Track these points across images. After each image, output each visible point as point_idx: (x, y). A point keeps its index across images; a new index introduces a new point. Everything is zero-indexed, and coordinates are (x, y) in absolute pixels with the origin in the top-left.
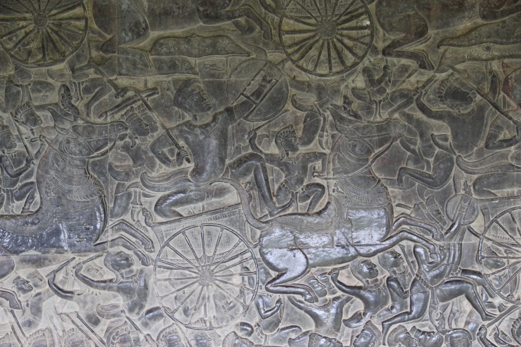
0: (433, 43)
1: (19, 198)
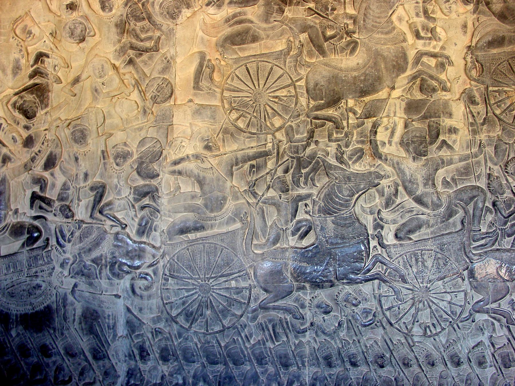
1: (509, 236)
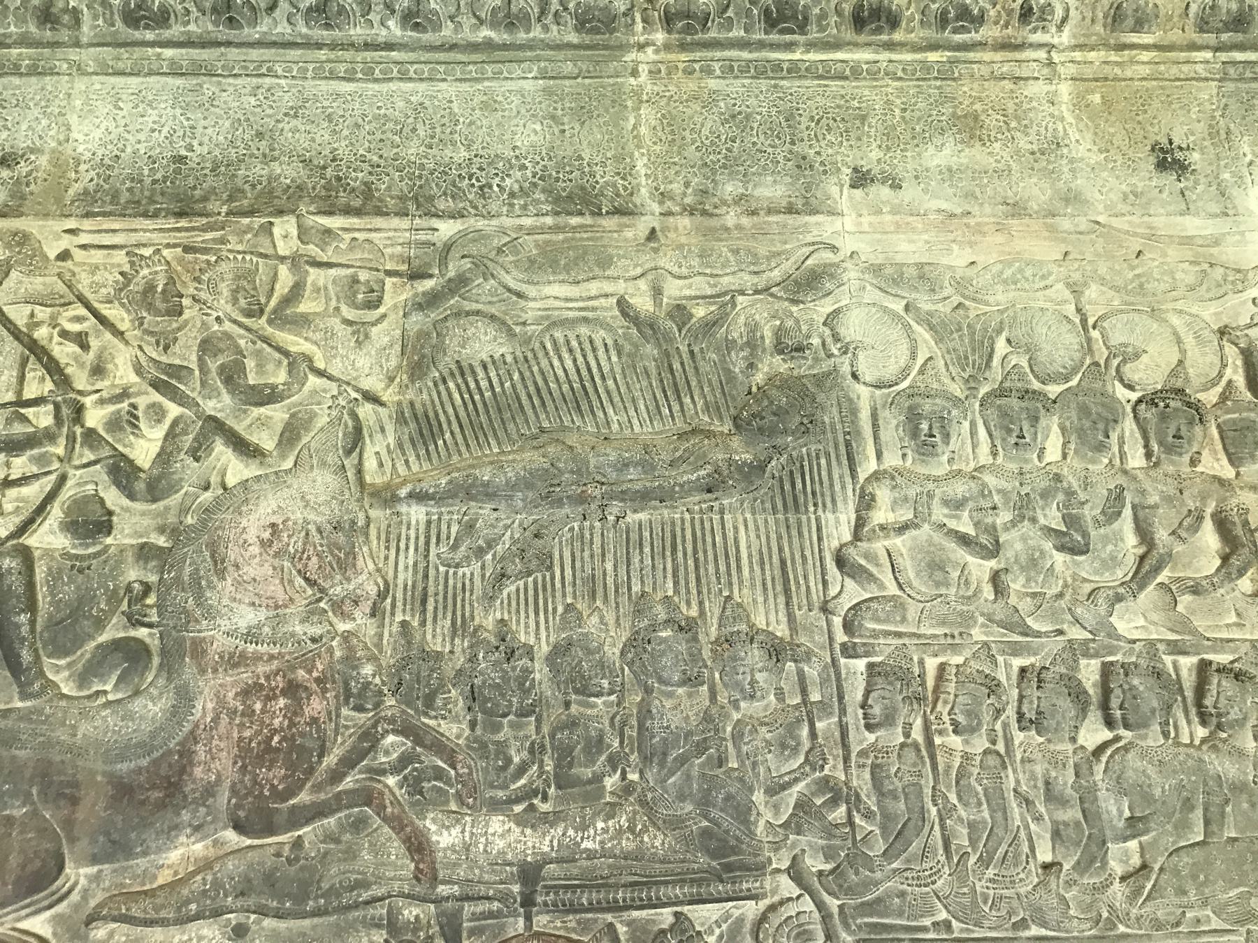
0: (76, 907)
